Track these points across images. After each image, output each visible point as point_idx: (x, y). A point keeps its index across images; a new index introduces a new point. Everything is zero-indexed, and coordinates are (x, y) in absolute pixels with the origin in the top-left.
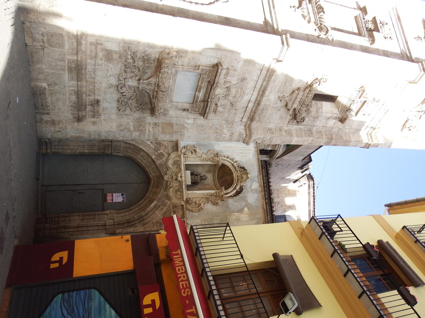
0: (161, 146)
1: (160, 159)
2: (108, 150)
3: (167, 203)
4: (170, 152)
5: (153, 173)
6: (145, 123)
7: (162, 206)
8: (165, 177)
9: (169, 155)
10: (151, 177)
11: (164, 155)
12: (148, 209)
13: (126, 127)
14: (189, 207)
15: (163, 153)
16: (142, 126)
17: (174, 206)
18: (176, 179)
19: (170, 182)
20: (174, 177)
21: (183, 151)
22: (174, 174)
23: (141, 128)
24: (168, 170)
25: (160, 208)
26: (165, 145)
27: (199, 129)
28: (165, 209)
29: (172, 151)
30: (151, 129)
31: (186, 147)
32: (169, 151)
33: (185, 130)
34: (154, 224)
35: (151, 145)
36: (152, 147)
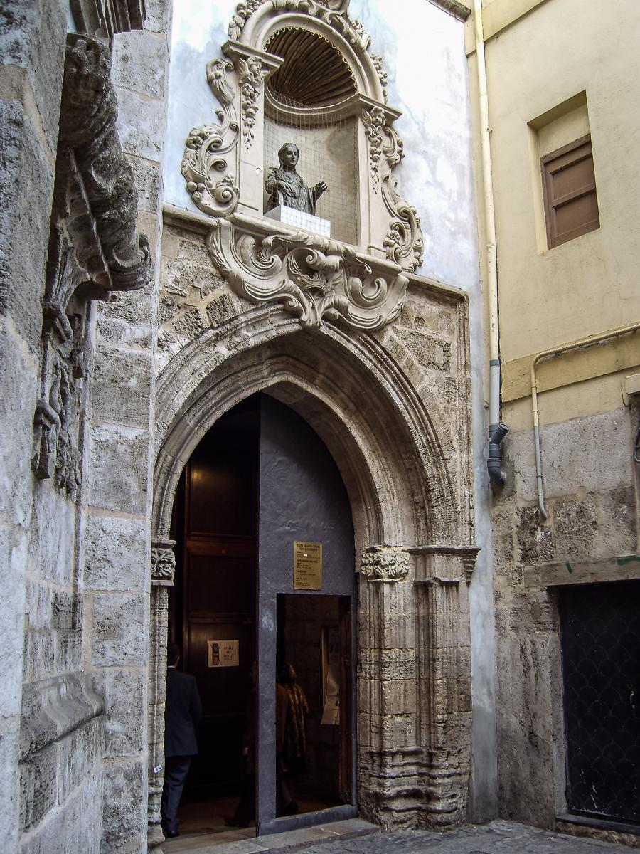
0: (180, 301)
1: (237, 322)
2: (164, 562)
3: (392, 339)
4: (213, 270)
5: (261, 371)
6: (105, 354)
7: (401, 365)
8: (309, 324)
9: (224, 276)
10: (276, 380)
11: (222, 298)
12: (407, 418)
13: (128, 458)
14: (407, 262)
15: (214, 303)
16: (121, 374)
17: (402, 319)
18: (327, 271)
19: (330, 307)
20: (317, 282)
21: (207, 200)
22: (306, 277)
23: (133, 382)
24: (282, 301)
25: (406, 371)
26: (176, 281)
27: (139, 78)
28: (410, 354)
29: (204, 255)
30: (139, 331)
31: (192, 183)
32: (206, 271)
33: (144, 154)
34: (451, 406)
35: (175, 348)
36: (182, 349)
